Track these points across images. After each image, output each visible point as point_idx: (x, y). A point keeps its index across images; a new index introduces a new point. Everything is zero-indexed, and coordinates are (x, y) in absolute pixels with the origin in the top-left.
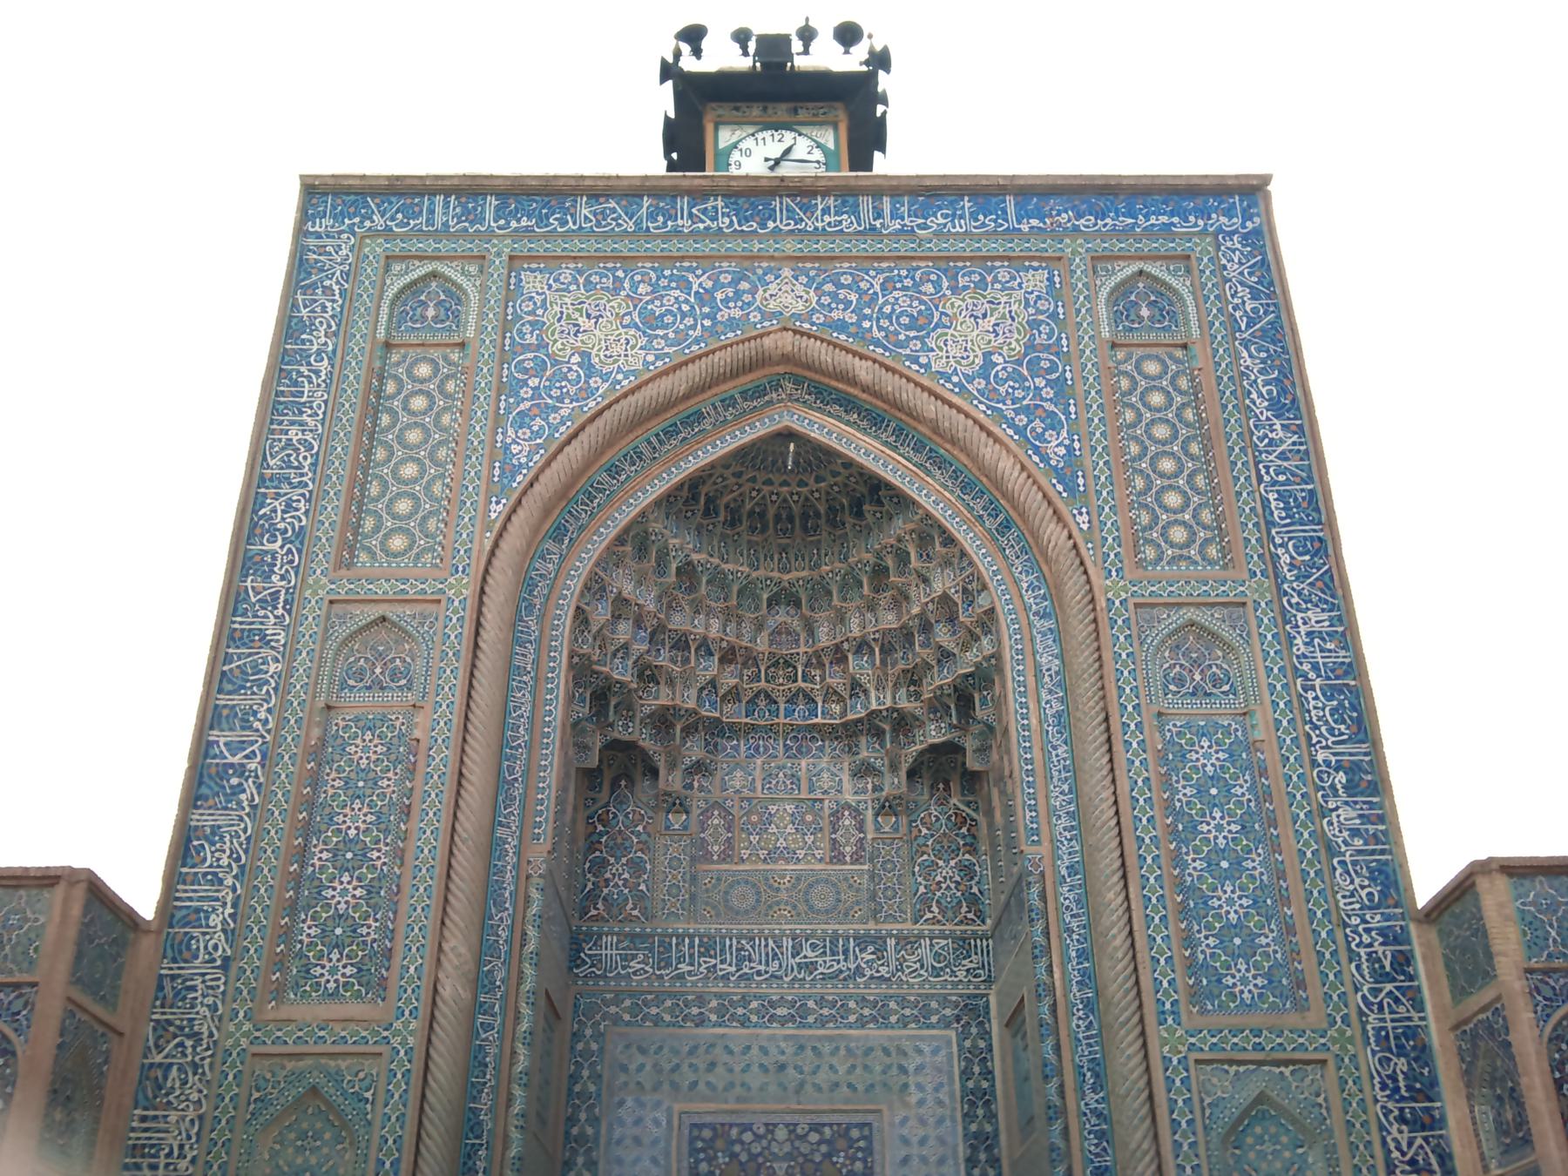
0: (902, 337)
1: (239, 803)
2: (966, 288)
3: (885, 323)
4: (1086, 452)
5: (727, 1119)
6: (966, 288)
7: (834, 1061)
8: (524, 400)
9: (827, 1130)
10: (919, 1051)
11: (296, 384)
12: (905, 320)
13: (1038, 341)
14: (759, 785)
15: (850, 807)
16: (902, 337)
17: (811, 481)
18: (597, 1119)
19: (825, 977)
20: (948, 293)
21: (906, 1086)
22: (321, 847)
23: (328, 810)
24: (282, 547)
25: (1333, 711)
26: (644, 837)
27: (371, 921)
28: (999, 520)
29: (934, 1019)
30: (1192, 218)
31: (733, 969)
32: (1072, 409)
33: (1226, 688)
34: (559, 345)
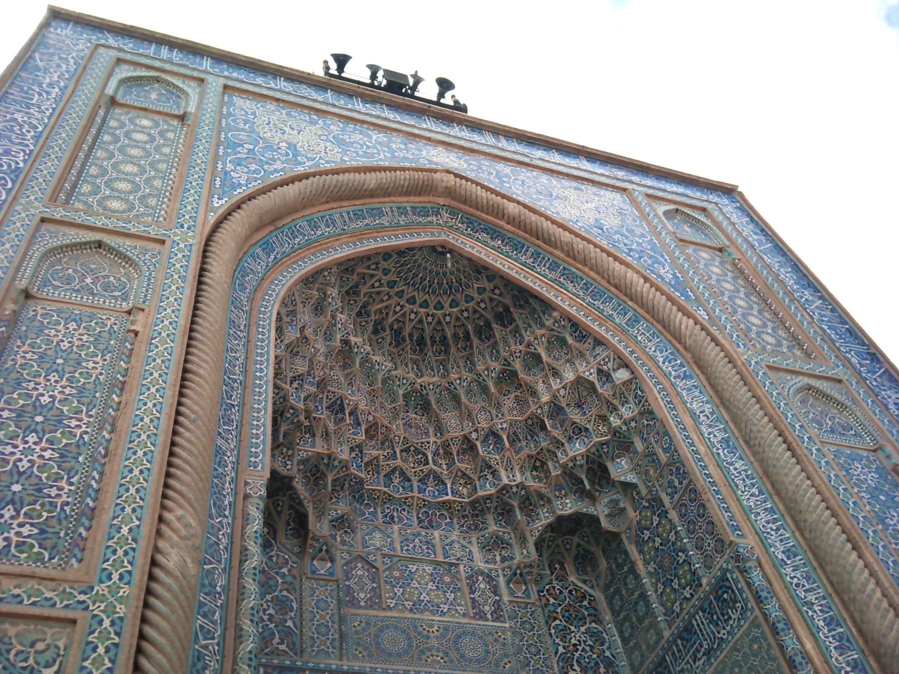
14: (398, 547)
15: (482, 573)
17: (447, 305)
26: (289, 579)
28: (628, 317)
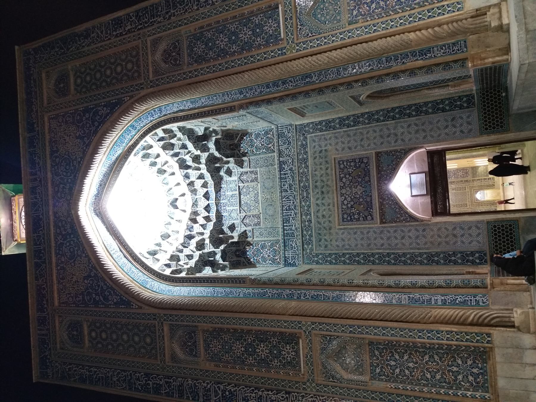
0: (73, 168)
1: (234, 391)
2: (57, 147)
3: (69, 174)
4: (105, 100)
5: (340, 210)
6: (57, 147)
7: (319, 175)
8: (100, 299)
9: (341, 176)
10: (315, 147)
11: (99, 379)
12: (68, 167)
13: (71, 121)
14: (235, 208)
16: (73, 168)
18: (343, 254)
19: (293, 181)
20: (59, 153)
21: (326, 150)
22: (248, 360)
23: (236, 359)
24: (151, 381)
25: (181, 5)
27: (271, 340)
28: (131, 129)
29: (304, 143)
30: (32, 72)
31: (293, 211)
32: (92, 106)
33: (177, 44)
34: (82, 288)
